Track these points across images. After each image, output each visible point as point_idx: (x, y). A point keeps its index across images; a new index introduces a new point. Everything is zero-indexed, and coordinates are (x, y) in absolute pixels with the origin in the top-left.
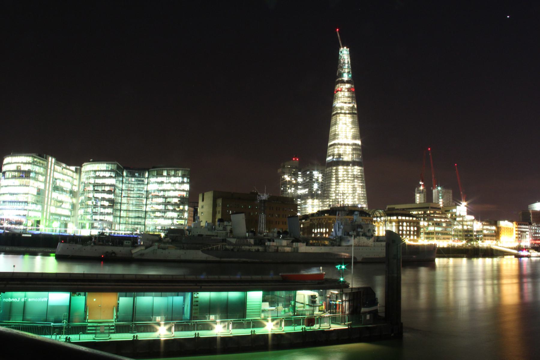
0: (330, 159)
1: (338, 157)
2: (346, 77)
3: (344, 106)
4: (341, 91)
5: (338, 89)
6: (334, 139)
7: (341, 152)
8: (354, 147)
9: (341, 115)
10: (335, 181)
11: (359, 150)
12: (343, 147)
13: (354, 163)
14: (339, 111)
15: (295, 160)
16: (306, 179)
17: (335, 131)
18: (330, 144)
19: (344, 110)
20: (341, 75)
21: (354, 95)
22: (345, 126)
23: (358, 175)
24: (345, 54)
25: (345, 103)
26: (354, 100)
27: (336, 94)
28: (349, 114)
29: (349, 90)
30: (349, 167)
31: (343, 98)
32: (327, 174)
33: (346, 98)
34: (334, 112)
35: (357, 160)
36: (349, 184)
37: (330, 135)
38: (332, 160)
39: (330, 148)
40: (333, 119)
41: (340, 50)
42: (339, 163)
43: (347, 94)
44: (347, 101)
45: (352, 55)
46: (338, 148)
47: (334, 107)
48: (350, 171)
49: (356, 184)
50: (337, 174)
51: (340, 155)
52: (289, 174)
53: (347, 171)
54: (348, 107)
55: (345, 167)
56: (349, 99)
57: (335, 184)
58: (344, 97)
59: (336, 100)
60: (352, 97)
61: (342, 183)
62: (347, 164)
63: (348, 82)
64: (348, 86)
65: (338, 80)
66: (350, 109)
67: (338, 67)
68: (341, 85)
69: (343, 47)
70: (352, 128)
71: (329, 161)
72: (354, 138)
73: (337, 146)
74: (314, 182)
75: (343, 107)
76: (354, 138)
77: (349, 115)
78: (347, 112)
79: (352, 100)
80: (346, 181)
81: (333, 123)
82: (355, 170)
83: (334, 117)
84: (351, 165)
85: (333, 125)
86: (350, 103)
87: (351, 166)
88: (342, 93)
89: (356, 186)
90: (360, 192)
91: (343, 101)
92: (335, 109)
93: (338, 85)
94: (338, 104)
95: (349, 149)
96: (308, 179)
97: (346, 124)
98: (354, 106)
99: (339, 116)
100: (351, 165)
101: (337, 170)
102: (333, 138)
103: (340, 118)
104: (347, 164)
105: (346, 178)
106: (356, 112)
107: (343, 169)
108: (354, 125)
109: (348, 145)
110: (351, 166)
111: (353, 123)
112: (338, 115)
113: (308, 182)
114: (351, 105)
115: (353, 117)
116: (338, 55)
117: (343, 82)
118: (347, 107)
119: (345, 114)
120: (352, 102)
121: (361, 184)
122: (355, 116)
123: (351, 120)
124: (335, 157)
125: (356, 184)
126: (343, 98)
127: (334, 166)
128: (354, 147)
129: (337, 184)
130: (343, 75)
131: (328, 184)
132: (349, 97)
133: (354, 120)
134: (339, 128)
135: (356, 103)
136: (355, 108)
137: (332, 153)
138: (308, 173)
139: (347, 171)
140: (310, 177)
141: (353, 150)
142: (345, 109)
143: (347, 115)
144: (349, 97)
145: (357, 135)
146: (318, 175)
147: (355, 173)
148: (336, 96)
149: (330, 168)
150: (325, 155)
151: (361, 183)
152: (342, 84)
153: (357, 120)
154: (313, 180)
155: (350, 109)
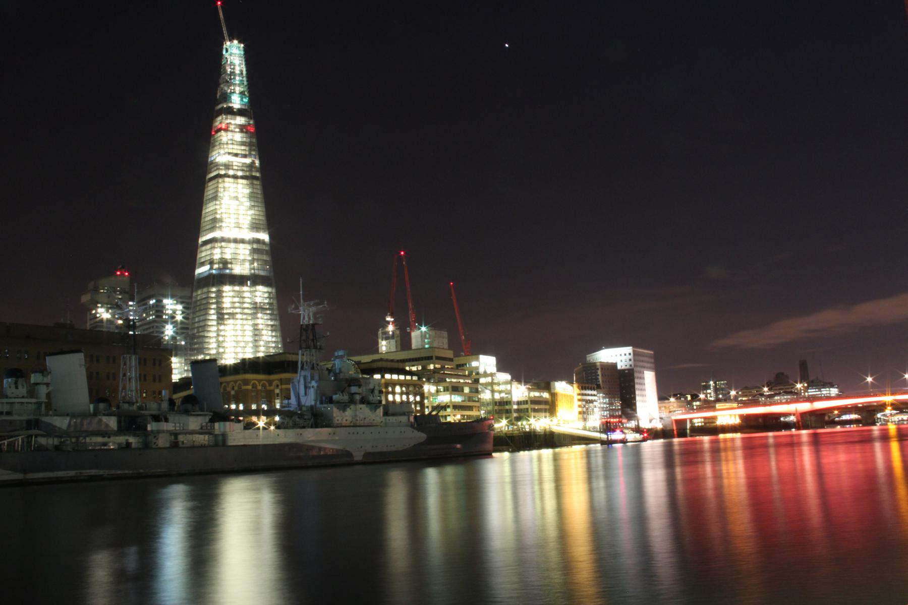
0: (204, 271)
1: (221, 265)
2: (237, 102)
3: (232, 162)
4: (226, 130)
5: (220, 126)
6: (213, 229)
7: (228, 256)
8: (255, 246)
9: (227, 179)
10: (214, 317)
11: (265, 253)
12: (232, 245)
13: (255, 280)
14: (222, 172)
15: (122, 274)
16: (148, 315)
17: (215, 212)
18: (202, 239)
19: (233, 169)
20: (226, 97)
21: (254, 140)
22: (237, 202)
23: (264, 304)
25: (236, 155)
26: (254, 150)
27: (216, 136)
28: (242, 177)
29: (242, 128)
30: (245, 288)
31: (231, 144)
32: (198, 303)
33: (237, 145)
34: (211, 172)
35: (262, 273)
36: (245, 322)
37: (202, 221)
38: (208, 273)
39: (204, 248)
40: (210, 188)
41: (225, 46)
42: (224, 278)
43: (238, 137)
44: (239, 152)
46: (221, 247)
47: (212, 163)
48: (247, 295)
49: (259, 321)
50: (219, 303)
51: (225, 263)
52: (109, 306)
53: (240, 295)
54: (243, 163)
55: (237, 288)
56: (243, 148)
57: (215, 323)
58: (233, 144)
59: (216, 148)
60: (250, 145)
61: (231, 321)
62: (240, 280)
63: (241, 113)
64: (241, 120)
65: (220, 106)
66: (245, 169)
67: (221, 81)
68: (226, 119)
69: (231, 40)
70: (252, 207)
71: (202, 276)
72: (255, 227)
73: (219, 245)
74: (166, 322)
75: (230, 164)
76: (255, 227)
77: (244, 182)
78: (240, 174)
79: (250, 150)
80: (239, 316)
81: (210, 197)
82: (258, 294)
83: (210, 184)
84: (249, 282)
85: (209, 199)
86: (245, 156)
87: (249, 285)
88: (230, 134)
89: (260, 327)
90: (270, 339)
91: (230, 151)
92: (215, 166)
93: (220, 118)
94: (221, 155)
95: (244, 251)
97: (236, 198)
98: (253, 162)
99: (224, 182)
100: (249, 282)
101: (219, 294)
102: (210, 227)
103: (226, 185)
104: (240, 280)
105: (238, 310)
106: (258, 175)
107: (234, 291)
108: (254, 201)
109: (243, 241)
110: (249, 285)
111: (252, 197)
112: (220, 180)
113: (153, 321)
114: (248, 161)
115: (252, 184)
116: (220, 56)
117: (230, 112)
118: (239, 164)
120: (250, 155)
121: (270, 323)
122: (255, 182)
123: (247, 191)
124: (216, 266)
125: (259, 321)
126: (231, 144)
127: (213, 285)
128: (255, 246)
129: (220, 322)
130: (230, 97)
131: (201, 324)
132: (243, 143)
133: (255, 191)
134: (222, 206)
135: (257, 157)
136: (256, 167)
137: (208, 258)
138: (152, 302)
139: (240, 295)
140: (157, 311)
142: (235, 168)
143: (240, 181)
144: (243, 143)
145: (261, 222)
146: (174, 307)
147: (258, 300)
148: (215, 141)
149: (205, 290)
150: (192, 261)
151: (271, 319)
152: (229, 117)
153: (259, 192)
154: (164, 317)
155: (245, 169)
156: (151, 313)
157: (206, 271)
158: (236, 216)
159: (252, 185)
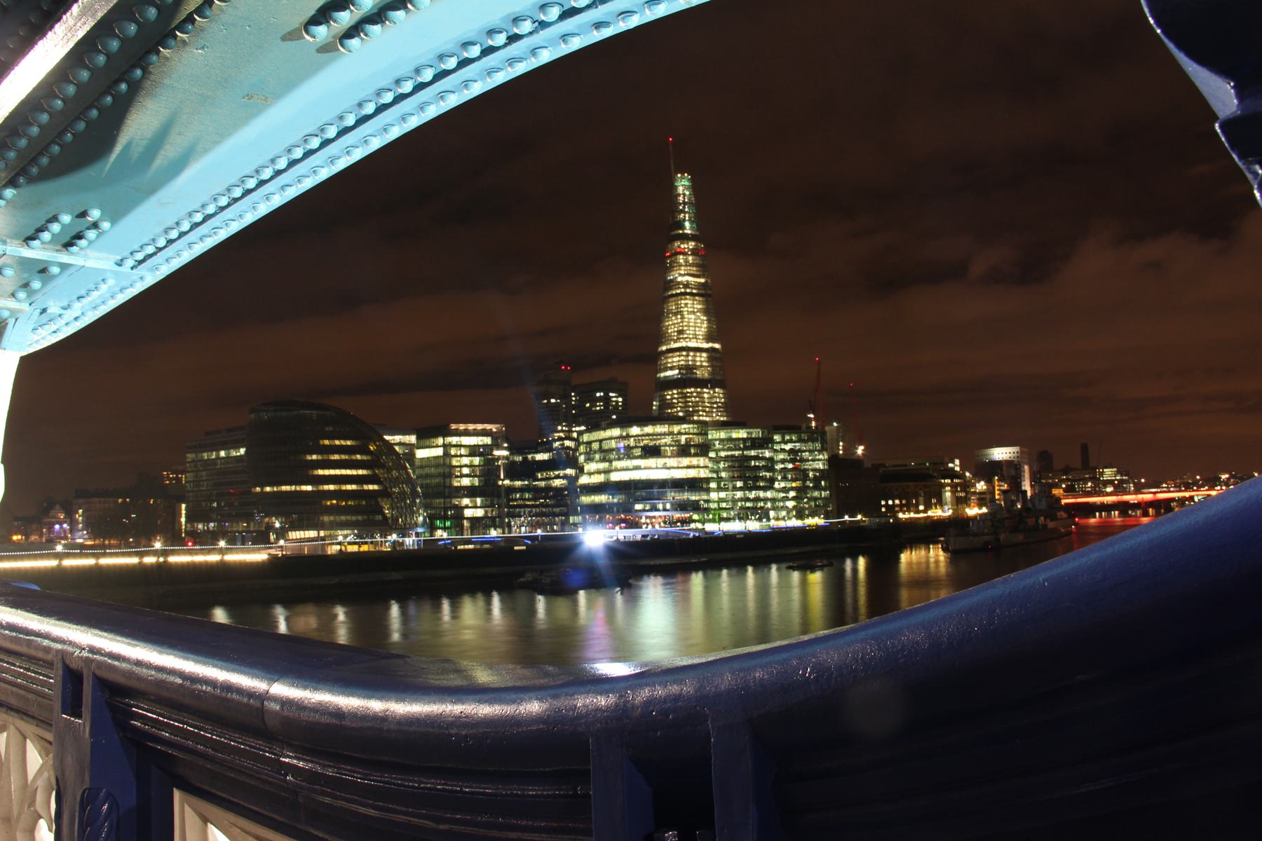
15: (566, 368)
20: (680, 225)
24: (683, 186)
29: (694, 252)
30: (705, 390)
45: (695, 188)
48: (706, 396)
53: (699, 395)
54: (699, 283)
56: (694, 269)
62: (701, 383)
64: (692, 244)
72: (709, 338)
76: (709, 338)
77: (701, 299)
78: (694, 291)
91: (689, 272)
92: (675, 285)
95: (702, 358)
96: (600, 406)
97: (693, 313)
98: (706, 282)
114: (703, 280)
117: (685, 238)
119: (691, 294)
122: (709, 299)
128: (713, 354)
141: (713, 360)
143: (697, 298)
156: (598, 404)
157: (673, 376)
158: (693, 329)
159: (706, 303)
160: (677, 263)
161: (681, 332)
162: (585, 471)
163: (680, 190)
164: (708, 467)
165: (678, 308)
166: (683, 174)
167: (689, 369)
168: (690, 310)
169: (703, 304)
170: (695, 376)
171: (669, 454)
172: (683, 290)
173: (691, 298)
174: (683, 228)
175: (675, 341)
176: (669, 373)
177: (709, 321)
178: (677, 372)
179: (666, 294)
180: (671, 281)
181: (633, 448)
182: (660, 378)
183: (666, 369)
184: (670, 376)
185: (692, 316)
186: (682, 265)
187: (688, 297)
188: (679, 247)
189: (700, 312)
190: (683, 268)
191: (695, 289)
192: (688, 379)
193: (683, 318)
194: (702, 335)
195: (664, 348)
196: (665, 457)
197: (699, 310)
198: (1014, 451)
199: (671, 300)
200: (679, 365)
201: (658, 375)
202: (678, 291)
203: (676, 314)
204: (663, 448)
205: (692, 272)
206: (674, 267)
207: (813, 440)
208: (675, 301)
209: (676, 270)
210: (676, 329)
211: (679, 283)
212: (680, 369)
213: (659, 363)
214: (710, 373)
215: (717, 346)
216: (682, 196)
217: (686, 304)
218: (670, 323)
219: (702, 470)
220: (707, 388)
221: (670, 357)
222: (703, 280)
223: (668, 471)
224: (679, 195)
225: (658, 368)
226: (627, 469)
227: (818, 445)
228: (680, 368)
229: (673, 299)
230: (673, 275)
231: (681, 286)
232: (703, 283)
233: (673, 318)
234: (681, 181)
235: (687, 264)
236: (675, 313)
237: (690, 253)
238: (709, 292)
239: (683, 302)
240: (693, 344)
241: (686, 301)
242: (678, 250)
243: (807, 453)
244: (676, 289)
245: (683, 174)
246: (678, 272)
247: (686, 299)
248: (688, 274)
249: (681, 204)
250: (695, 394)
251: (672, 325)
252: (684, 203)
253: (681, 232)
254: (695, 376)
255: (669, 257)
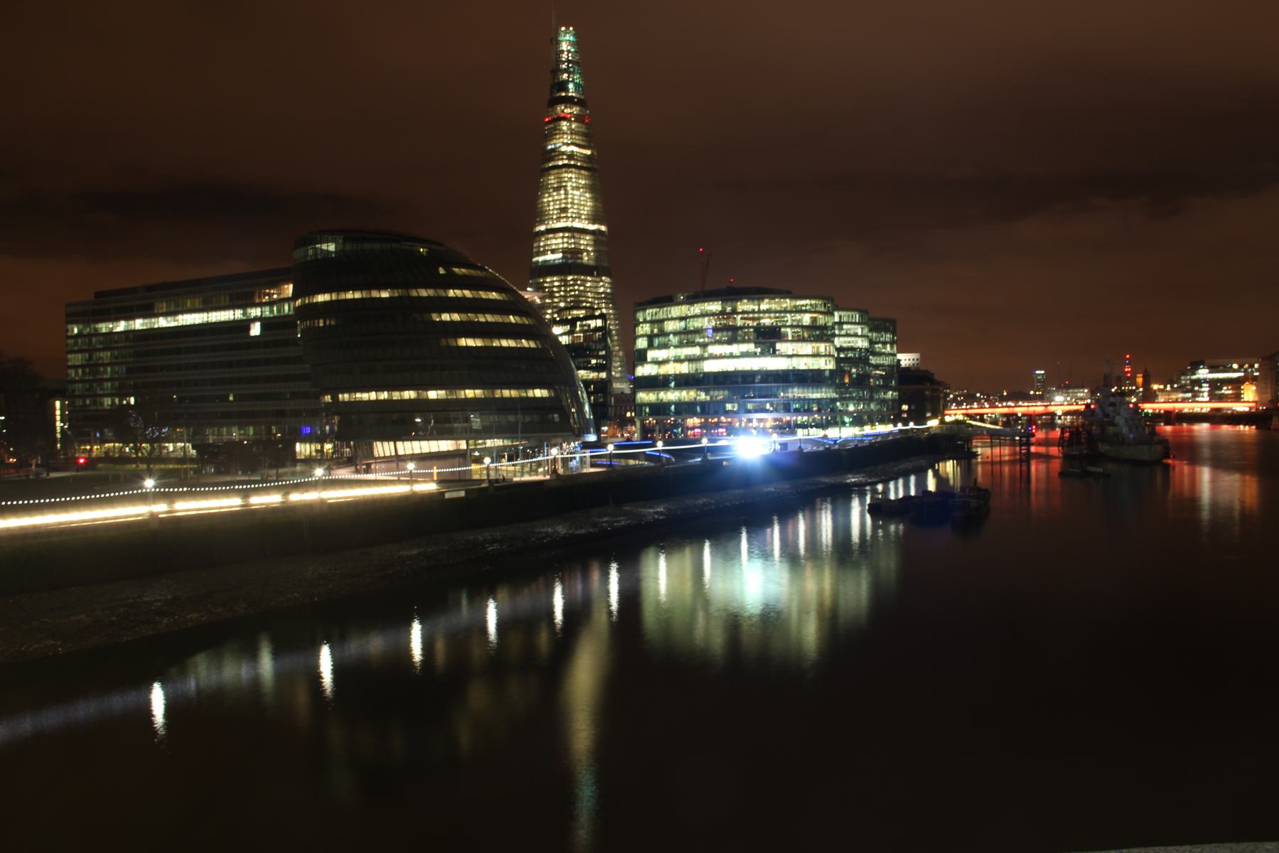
20: (563, 86)
24: (567, 41)
30: (589, 278)
54: (585, 154)
56: (580, 138)
60: (585, 135)
64: (575, 110)
71: (548, 264)
72: (594, 219)
84: (595, 273)
95: (585, 242)
97: (577, 188)
98: (592, 154)
100: (595, 273)
114: (588, 152)
117: (569, 101)
118: (582, 156)
119: (575, 166)
128: (600, 237)
143: (583, 172)
155: (586, 160)
157: (555, 260)
159: (591, 177)
160: (560, 130)
161: (564, 210)
162: (649, 360)
163: (564, 46)
164: (833, 356)
165: (561, 182)
166: (567, 28)
167: (576, 252)
168: (574, 185)
169: (589, 180)
170: (580, 261)
171: (790, 338)
172: (566, 162)
173: (577, 171)
174: (567, 90)
175: (558, 219)
176: (550, 257)
177: (594, 199)
178: (560, 255)
179: (546, 166)
180: (553, 150)
181: (742, 328)
182: (537, 262)
183: (544, 253)
184: (549, 261)
185: (577, 193)
186: (564, 133)
187: (573, 170)
188: (563, 111)
189: (586, 188)
190: (565, 136)
191: (581, 161)
192: (570, 265)
193: (566, 194)
194: (588, 214)
195: (543, 228)
196: (787, 341)
197: (585, 186)
198: (913, 357)
199: (552, 172)
200: (562, 248)
201: (535, 259)
202: (560, 163)
203: (558, 189)
204: (783, 330)
205: (578, 142)
206: (556, 134)
207: (887, 330)
208: (558, 173)
209: (559, 138)
210: (557, 207)
211: (563, 153)
212: (563, 252)
213: (535, 245)
214: (597, 259)
215: (603, 228)
216: (566, 53)
217: (571, 178)
218: (550, 199)
219: (823, 360)
220: (592, 275)
221: (551, 238)
222: (588, 152)
223: (790, 359)
224: (562, 52)
225: (534, 250)
226: (731, 356)
227: (888, 337)
228: (565, 251)
229: (556, 171)
230: (555, 144)
231: (565, 157)
232: (589, 156)
233: (555, 194)
234: (565, 36)
235: (573, 132)
236: (557, 187)
237: (573, 119)
238: (595, 166)
239: (566, 175)
240: (577, 224)
241: (570, 175)
242: (562, 115)
243: (880, 345)
244: (559, 160)
245: (567, 28)
246: (561, 140)
247: (571, 172)
248: (572, 144)
249: (564, 62)
250: (579, 282)
251: (551, 201)
252: (569, 61)
253: (564, 94)
254: (580, 261)
255: (550, 122)
